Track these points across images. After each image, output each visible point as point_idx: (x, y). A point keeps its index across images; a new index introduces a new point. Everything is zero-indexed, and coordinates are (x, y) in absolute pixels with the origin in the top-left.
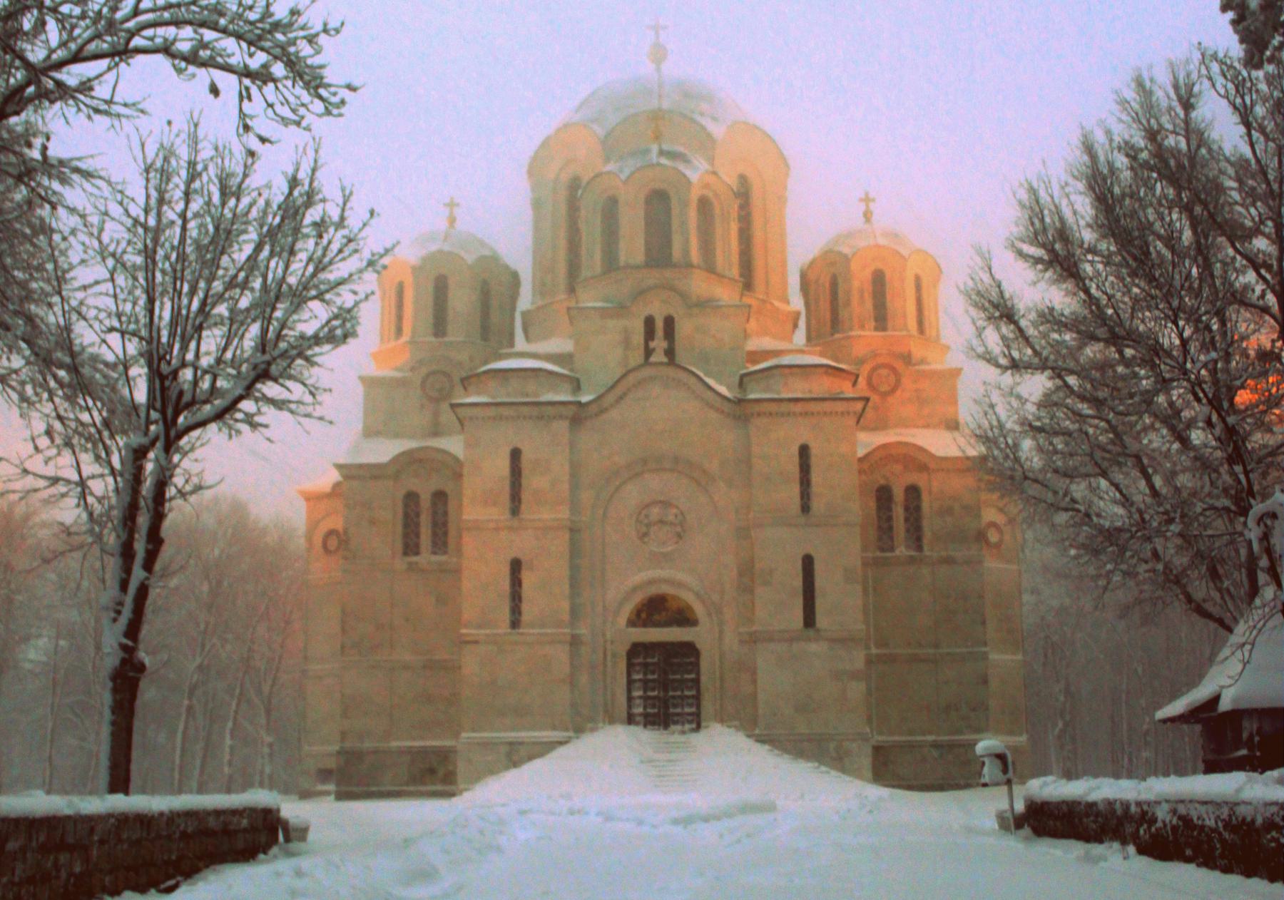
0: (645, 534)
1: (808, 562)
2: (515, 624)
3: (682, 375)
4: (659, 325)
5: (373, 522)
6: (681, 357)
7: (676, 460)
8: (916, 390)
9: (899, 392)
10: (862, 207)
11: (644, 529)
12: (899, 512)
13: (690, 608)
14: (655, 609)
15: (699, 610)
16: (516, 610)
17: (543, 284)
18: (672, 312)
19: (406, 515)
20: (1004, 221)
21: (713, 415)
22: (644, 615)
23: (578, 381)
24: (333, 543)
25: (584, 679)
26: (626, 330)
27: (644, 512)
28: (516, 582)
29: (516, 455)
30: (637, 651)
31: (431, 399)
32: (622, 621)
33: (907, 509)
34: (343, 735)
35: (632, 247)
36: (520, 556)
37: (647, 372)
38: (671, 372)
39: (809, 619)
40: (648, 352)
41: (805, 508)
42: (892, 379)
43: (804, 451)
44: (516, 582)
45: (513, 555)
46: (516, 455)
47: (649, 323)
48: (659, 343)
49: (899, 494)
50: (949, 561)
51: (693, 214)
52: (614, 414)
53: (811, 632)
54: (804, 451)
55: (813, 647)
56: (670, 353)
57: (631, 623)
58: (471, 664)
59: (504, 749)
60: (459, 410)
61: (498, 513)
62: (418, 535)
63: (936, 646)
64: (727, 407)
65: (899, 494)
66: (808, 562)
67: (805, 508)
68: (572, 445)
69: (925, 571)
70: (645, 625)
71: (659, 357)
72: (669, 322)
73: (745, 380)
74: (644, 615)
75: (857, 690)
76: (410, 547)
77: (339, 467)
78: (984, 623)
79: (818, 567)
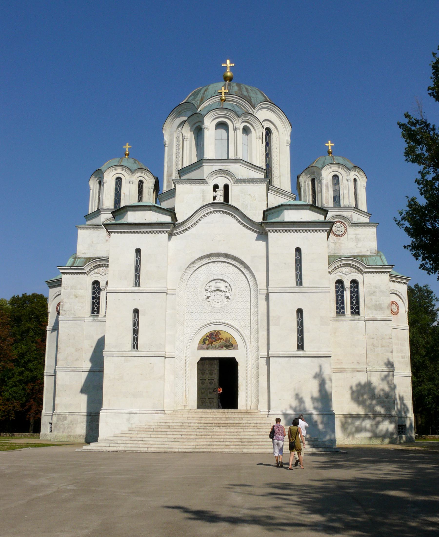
0: (208, 297)
1: (300, 312)
2: (135, 346)
12: (347, 295)
14: (212, 339)
16: (135, 339)
18: (227, 182)
22: (207, 342)
26: (203, 192)
27: (209, 285)
28: (136, 324)
29: (138, 251)
30: (203, 361)
33: (351, 292)
39: (301, 346)
41: (299, 282)
42: (343, 229)
43: (298, 250)
44: (136, 324)
46: (138, 251)
47: (216, 187)
48: (220, 195)
49: (347, 284)
50: (374, 320)
53: (301, 353)
54: (298, 250)
57: (200, 348)
59: (126, 416)
60: (106, 227)
65: (347, 284)
66: (300, 312)
67: (299, 282)
70: (208, 349)
72: (226, 187)
73: (266, 213)
78: (392, 352)
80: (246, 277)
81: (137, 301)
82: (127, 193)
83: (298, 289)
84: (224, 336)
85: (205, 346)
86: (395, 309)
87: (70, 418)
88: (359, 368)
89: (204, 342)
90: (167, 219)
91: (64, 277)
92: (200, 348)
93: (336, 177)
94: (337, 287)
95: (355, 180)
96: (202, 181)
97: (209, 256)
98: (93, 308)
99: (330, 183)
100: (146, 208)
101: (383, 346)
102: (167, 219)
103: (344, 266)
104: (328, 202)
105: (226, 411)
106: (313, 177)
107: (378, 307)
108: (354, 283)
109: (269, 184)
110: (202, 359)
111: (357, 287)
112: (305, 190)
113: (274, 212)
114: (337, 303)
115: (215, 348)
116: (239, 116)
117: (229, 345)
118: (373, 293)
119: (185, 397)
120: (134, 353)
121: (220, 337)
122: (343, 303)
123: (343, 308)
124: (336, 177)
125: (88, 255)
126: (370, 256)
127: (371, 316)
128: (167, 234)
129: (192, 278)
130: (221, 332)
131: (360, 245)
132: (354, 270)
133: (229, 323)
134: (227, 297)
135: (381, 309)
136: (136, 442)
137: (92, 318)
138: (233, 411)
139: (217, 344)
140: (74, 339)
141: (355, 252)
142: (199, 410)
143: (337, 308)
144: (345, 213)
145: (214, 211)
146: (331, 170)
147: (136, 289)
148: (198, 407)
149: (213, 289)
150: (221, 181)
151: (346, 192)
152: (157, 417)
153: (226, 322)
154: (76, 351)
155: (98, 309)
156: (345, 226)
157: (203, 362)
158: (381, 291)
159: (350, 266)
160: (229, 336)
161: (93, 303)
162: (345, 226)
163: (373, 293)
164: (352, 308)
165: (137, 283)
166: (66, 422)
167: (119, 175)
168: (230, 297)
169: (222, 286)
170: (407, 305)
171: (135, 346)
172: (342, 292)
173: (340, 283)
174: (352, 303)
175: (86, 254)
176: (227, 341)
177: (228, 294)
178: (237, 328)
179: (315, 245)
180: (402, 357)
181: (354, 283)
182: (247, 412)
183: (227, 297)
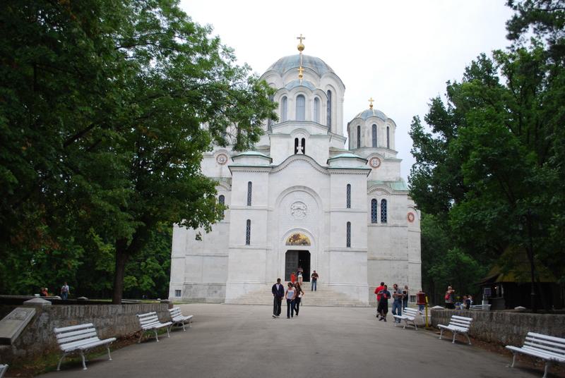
1: (349, 224)
2: (248, 242)
3: (309, 160)
4: (300, 141)
6: (307, 153)
7: (305, 187)
8: (387, 167)
9: (380, 168)
10: (370, 103)
15: (311, 240)
20: (424, 111)
29: (250, 183)
32: (285, 242)
33: (382, 207)
34: (185, 278)
37: (296, 157)
38: (304, 158)
39: (349, 245)
40: (296, 151)
41: (349, 206)
42: (378, 163)
43: (349, 186)
46: (250, 183)
47: (297, 140)
48: (300, 148)
49: (379, 202)
50: (396, 226)
51: (312, 103)
52: (284, 171)
53: (349, 249)
54: (349, 186)
55: (348, 254)
56: (303, 151)
57: (287, 244)
58: (232, 255)
63: (391, 255)
64: (323, 170)
65: (379, 202)
66: (349, 224)
67: (349, 206)
68: (269, 181)
69: (388, 228)
70: (292, 245)
71: (300, 152)
72: (303, 140)
75: (364, 269)
83: (348, 209)
84: (302, 237)
86: (411, 217)
87: (194, 287)
88: (385, 257)
89: (290, 241)
90: (267, 163)
92: (287, 244)
93: (374, 126)
94: (372, 204)
95: (388, 128)
96: (287, 136)
97: (294, 187)
99: (371, 130)
101: (401, 244)
102: (267, 163)
103: (377, 190)
104: (368, 144)
107: (400, 218)
108: (384, 201)
109: (330, 130)
110: (288, 251)
111: (386, 204)
112: (353, 134)
114: (372, 214)
116: (312, 91)
117: (305, 243)
118: (396, 208)
120: (248, 246)
122: (376, 214)
123: (376, 218)
124: (374, 126)
126: (396, 182)
127: (394, 223)
131: (389, 174)
132: (384, 193)
135: (401, 219)
139: (298, 241)
141: (386, 179)
143: (372, 218)
144: (380, 152)
149: (296, 208)
151: (381, 136)
156: (380, 161)
157: (289, 253)
158: (403, 207)
159: (382, 190)
160: (305, 237)
162: (380, 161)
163: (396, 208)
164: (382, 218)
165: (249, 203)
166: (192, 290)
169: (301, 206)
170: (420, 216)
171: (248, 242)
172: (376, 207)
173: (374, 201)
174: (382, 214)
176: (304, 240)
179: (360, 185)
180: (416, 250)
181: (384, 201)
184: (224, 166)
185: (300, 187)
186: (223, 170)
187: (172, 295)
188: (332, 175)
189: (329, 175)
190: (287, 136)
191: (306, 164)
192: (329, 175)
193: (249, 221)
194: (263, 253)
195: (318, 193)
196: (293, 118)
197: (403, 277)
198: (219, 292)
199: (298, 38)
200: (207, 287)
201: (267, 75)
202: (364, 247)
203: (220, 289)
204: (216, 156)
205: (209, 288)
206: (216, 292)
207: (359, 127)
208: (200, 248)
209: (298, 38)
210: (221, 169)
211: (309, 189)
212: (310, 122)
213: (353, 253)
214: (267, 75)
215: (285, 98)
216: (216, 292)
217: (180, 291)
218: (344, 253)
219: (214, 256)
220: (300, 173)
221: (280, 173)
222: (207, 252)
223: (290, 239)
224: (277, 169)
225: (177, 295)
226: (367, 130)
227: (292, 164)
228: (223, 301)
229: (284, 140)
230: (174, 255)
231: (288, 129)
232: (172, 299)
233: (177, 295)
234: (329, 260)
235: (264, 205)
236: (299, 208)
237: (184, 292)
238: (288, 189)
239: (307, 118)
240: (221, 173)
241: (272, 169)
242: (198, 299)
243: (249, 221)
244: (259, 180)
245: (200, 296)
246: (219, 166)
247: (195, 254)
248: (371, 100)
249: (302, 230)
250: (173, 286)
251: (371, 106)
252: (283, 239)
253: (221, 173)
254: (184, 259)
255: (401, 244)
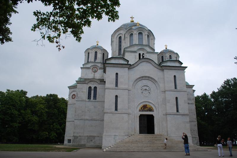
1: (177, 98)
2: (116, 109)
5: (82, 92)
7: (149, 77)
11: (142, 91)
13: (152, 107)
14: (144, 108)
17: (114, 54)
19: (89, 91)
21: (156, 69)
22: (142, 109)
23: (129, 61)
24: (74, 97)
25: (130, 122)
29: (117, 74)
31: (93, 72)
34: (74, 133)
35: (136, 40)
36: (118, 95)
39: (177, 111)
41: (176, 88)
43: (175, 76)
45: (115, 95)
46: (117, 74)
47: (140, 54)
54: (175, 76)
55: (178, 116)
57: (140, 111)
58: (106, 117)
61: (114, 86)
62: (91, 95)
66: (177, 98)
67: (176, 88)
68: (128, 73)
70: (143, 111)
74: (142, 109)
76: (89, 97)
77: (76, 81)
79: (179, 99)
80: (156, 85)
81: (117, 92)
82: (99, 57)
83: (175, 90)
85: (142, 110)
91: (78, 84)
92: (140, 111)
93: (170, 56)
95: (176, 57)
96: (135, 52)
97: (142, 77)
98: (88, 97)
100: (120, 58)
101: (192, 113)
105: (149, 135)
106: (162, 55)
110: (141, 115)
113: (165, 63)
115: (145, 111)
117: (151, 110)
119: (135, 129)
120: (116, 112)
121: (147, 107)
125: (85, 78)
128: (127, 68)
129: (136, 85)
130: (148, 105)
133: (151, 102)
134: (149, 93)
135: (191, 100)
136: (127, 147)
137: (88, 100)
138: (154, 135)
139: (146, 109)
140: (81, 107)
142: (143, 135)
145: (144, 61)
146: (169, 54)
147: (117, 88)
148: (140, 133)
149: (144, 89)
150: (141, 53)
152: (126, 137)
153: (150, 101)
154: (82, 112)
155: (91, 97)
157: (141, 116)
158: (190, 94)
161: (88, 95)
165: (117, 85)
166: (78, 139)
167: (96, 51)
168: (151, 92)
169: (147, 88)
171: (116, 109)
175: (84, 77)
176: (150, 108)
177: (149, 91)
178: (154, 104)
182: (158, 135)
183: (149, 93)
184: (96, 73)
185: (146, 77)
186: (96, 75)
187: (66, 142)
188: (165, 70)
189: (163, 70)
190: (135, 52)
191: (149, 64)
192: (163, 70)
193: (116, 96)
194: (125, 116)
195: (156, 79)
196: (137, 43)
197: (194, 131)
198: (93, 141)
199: (131, 18)
200: (87, 138)
201: (118, 30)
202: (187, 112)
203: (94, 139)
204: (91, 68)
205: (88, 139)
206: (92, 141)
207: (162, 57)
208: (82, 115)
209: (131, 18)
210: (94, 75)
211: (152, 78)
212: (146, 45)
213: (181, 116)
214: (118, 30)
215: (132, 35)
216: (92, 141)
217: (71, 140)
218: (175, 116)
219: (91, 120)
220: (145, 69)
221: (134, 68)
222: (87, 117)
223: (141, 108)
224: (133, 66)
225: (69, 142)
226: (167, 57)
227: (141, 64)
228: (100, 147)
229: (133, 54)
230: (68, 119)
231: (135, 49)
232: (66, 145)
233: (69, 142)
234: (167, 120)
235: (126, 87)
236: (146, 90)
237: (73, 141)
238: (139, 78)
239: (144, 43)
240: (94, 76)
241: (130, 67)
242: (81, 145)
243: (116, 96)
244: (123, 72)
245: (83, 143)
246: (93, 73)
247: (80, 119)
248: (166, 46)
249: (149, 102)
250: (66, 138)
251: (166, 48)
252: (137, 108)
253: (94, 76)
254: (74, 122)
255: (192, 113)
